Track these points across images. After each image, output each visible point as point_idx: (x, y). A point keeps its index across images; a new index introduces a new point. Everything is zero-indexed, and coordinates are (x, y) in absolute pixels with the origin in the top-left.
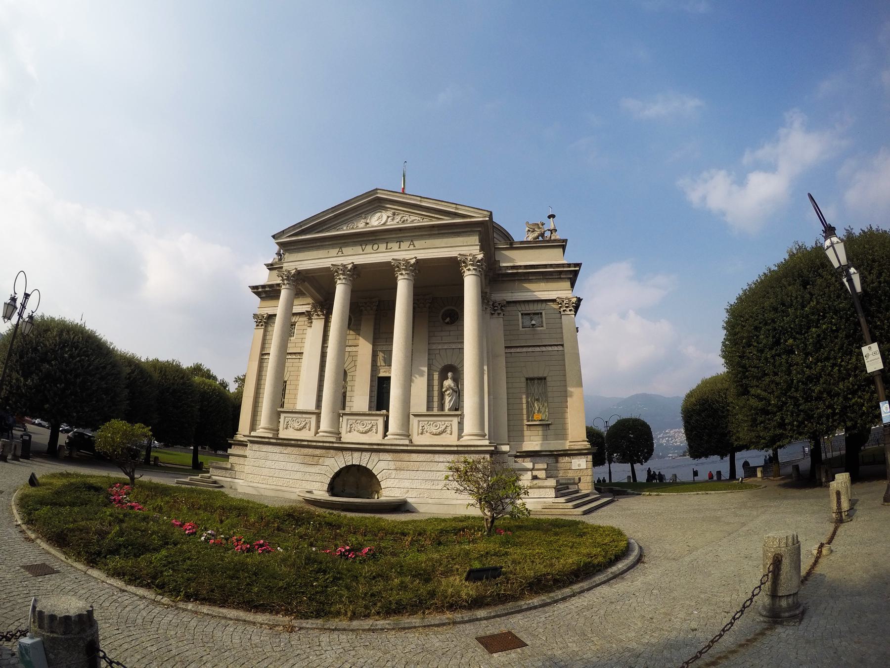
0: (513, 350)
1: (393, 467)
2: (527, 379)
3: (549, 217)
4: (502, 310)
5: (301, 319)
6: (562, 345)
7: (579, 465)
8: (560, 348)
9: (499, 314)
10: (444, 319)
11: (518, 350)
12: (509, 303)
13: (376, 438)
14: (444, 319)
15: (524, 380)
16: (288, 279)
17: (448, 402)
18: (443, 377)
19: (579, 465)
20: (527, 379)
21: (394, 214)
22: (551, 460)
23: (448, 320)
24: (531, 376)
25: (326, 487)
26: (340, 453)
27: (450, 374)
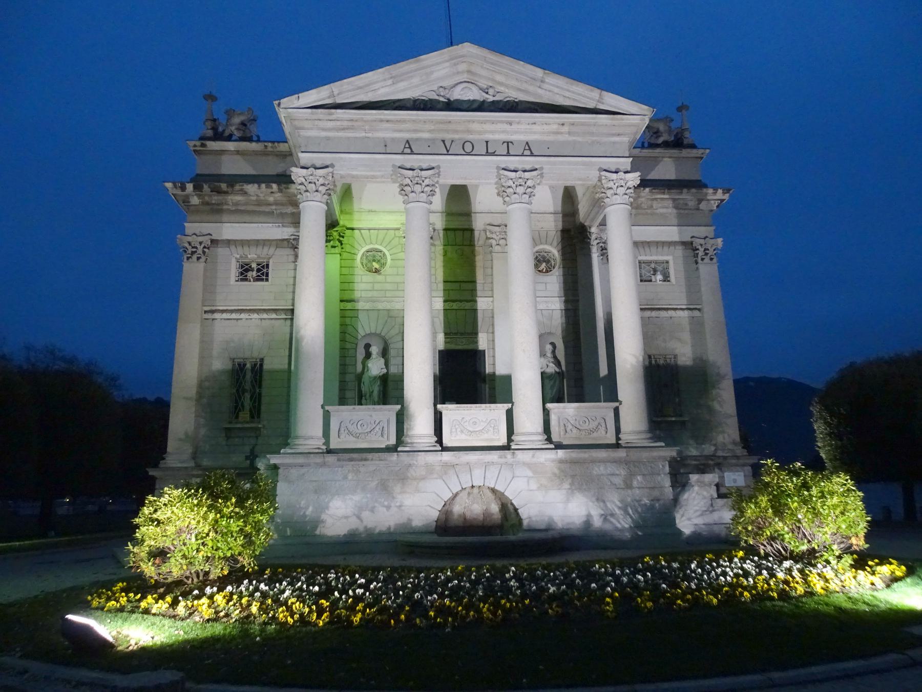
3: (680, 109)
5: (280, 252)
6: (699, 310)
7: (735, 481)
8: (697, 313)
19: (735, 481)
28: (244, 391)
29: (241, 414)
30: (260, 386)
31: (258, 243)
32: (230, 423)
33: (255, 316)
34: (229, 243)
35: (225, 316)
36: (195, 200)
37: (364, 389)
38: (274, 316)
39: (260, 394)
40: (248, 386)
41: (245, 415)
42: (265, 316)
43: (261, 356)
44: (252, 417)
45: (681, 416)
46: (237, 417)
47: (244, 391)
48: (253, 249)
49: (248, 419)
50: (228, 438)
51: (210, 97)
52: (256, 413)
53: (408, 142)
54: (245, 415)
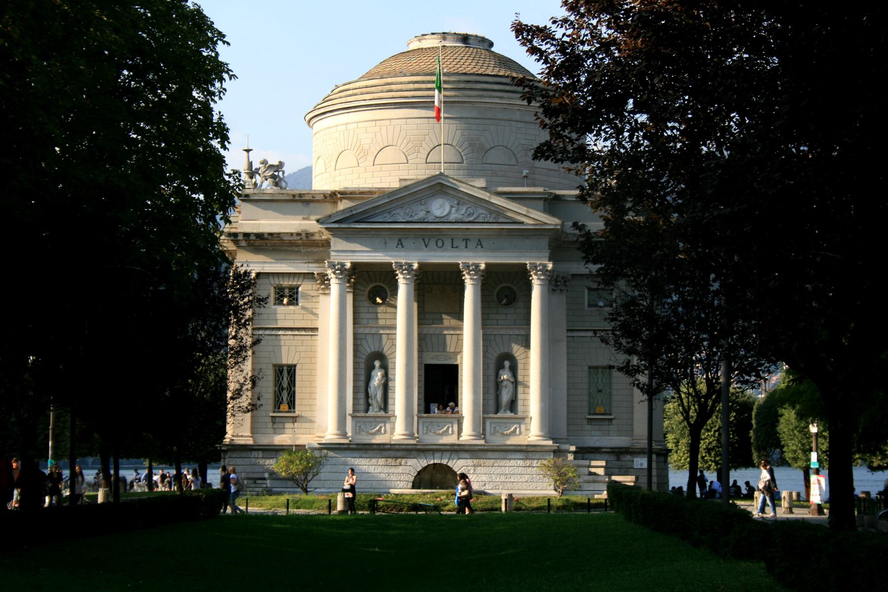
0: (575, 334)
1: (471, 464)
2: (590, 368)
4: (565, 285)
7: (642, 464)
9: (561, 290)
10: (500, 301)
11: (582, 334)
12: (574, 276)
13: (451, 439)
14: (500, 301)
15: (586, 368)
16: (341, 274)
17: (505, 397)
18: (500, 367)
19: (642, 464)
20: (590, 368)
21: (458, 204)
22: (612, 458)
23: (504, 301)
24: (595, 364)
25: (410, 485)
26: (422, 454)
27: (507, 364)
28: (283, 389)
29: (282, 407)
30: (294, 386)
31: (289, 275)
32: (274, 412)
33: (290, 333)
34: (268, 274)
35: (267, 332)
36: (243, 244)
37: (371, 391)
38: (303, 333)
39: (294, 392)
40: (285, 385)
41: (284, 407)
42: (297, 333)
43: (294, 363)
44: (290, 408)
45: (610, 414)
46: (279, 408)
47: (283, 389)
48: (286, 279)
49: (287, 409)
50: (274, 423)
51: (248, 151)
52: (292, 405)
53: (400, 240)
54: (284, 407)
